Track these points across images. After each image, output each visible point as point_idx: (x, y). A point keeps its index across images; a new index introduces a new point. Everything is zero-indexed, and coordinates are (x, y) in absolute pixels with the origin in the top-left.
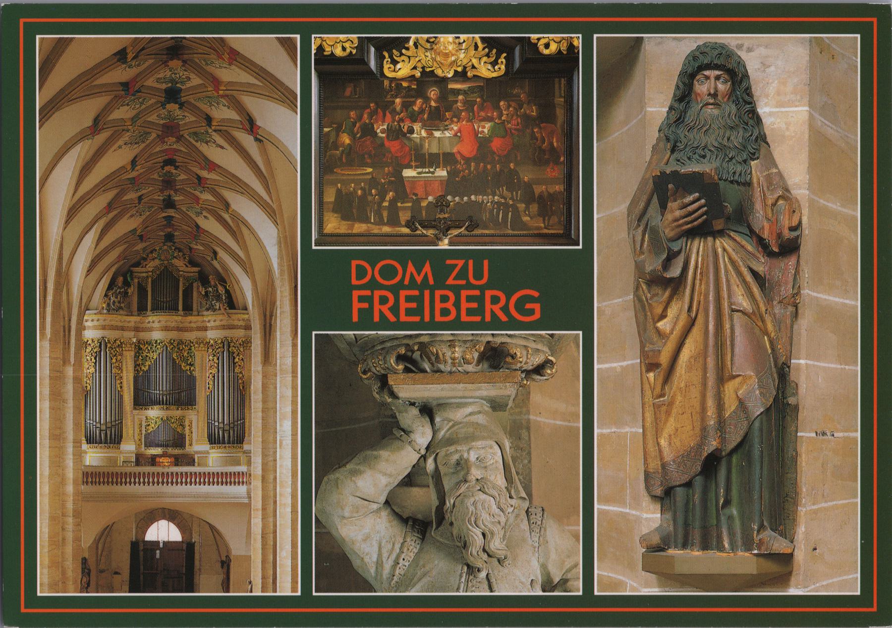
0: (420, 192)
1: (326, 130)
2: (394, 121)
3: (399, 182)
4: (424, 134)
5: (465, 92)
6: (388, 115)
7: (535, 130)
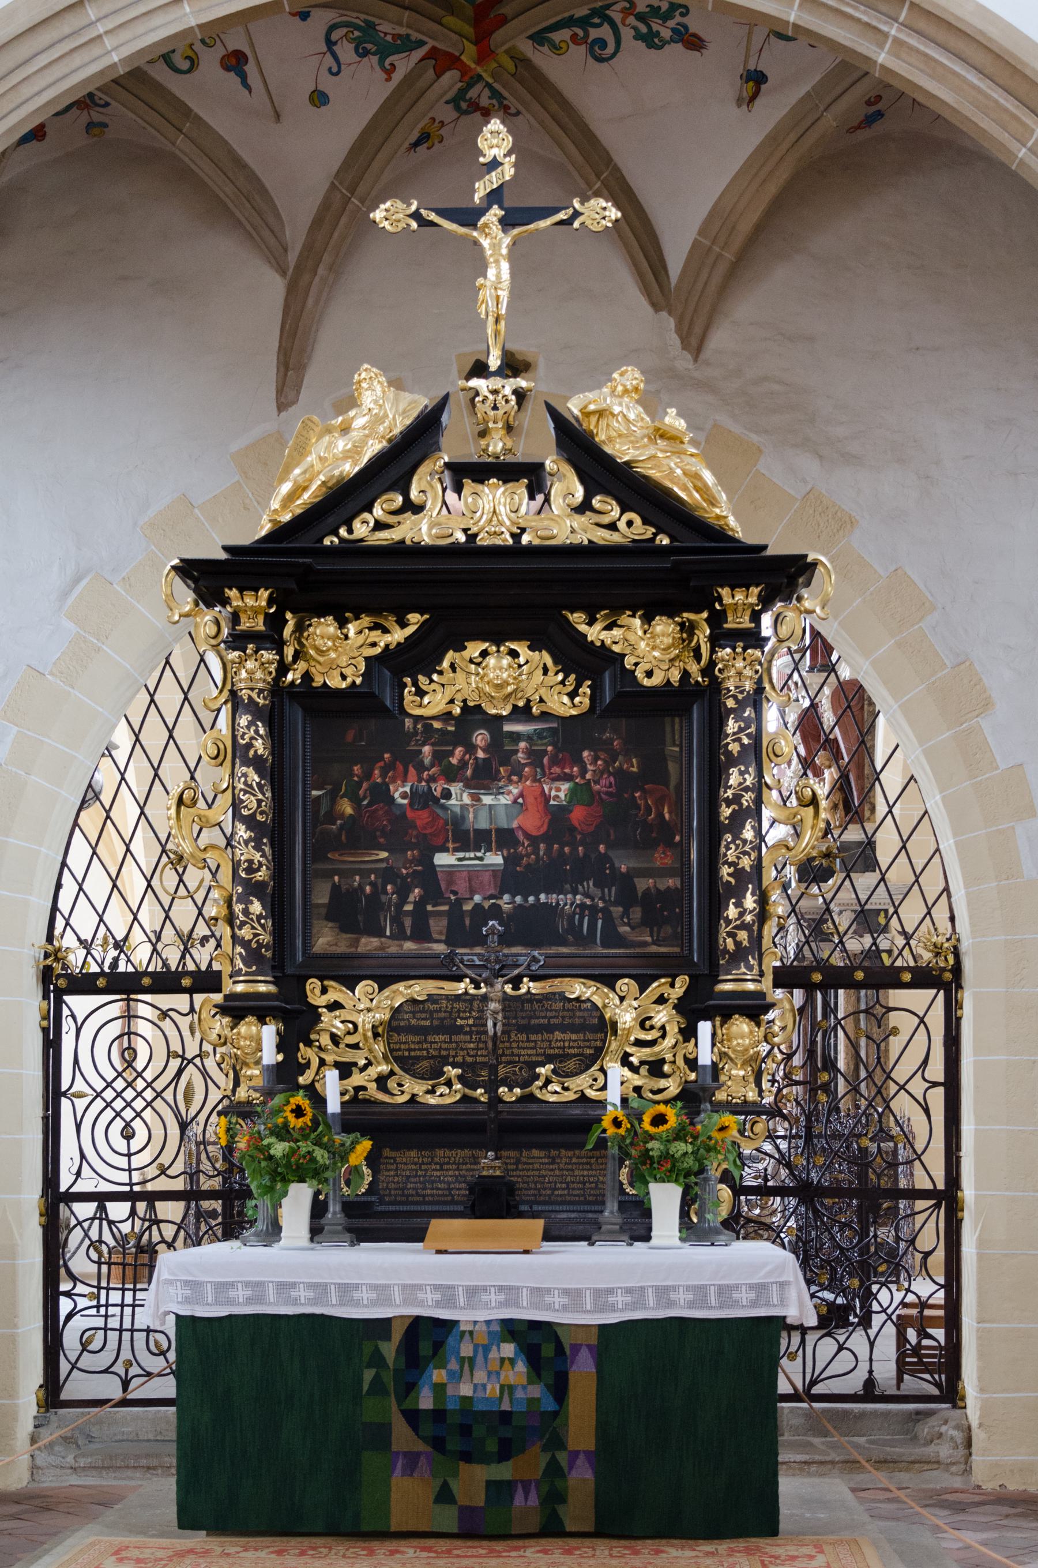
0: (462, 887)
1: (315, 793)
2: (420, 780)
3: (429, 875)
4: (467, 799)
5: (529, 738)
6: (412, 771)
7: (637, 795)
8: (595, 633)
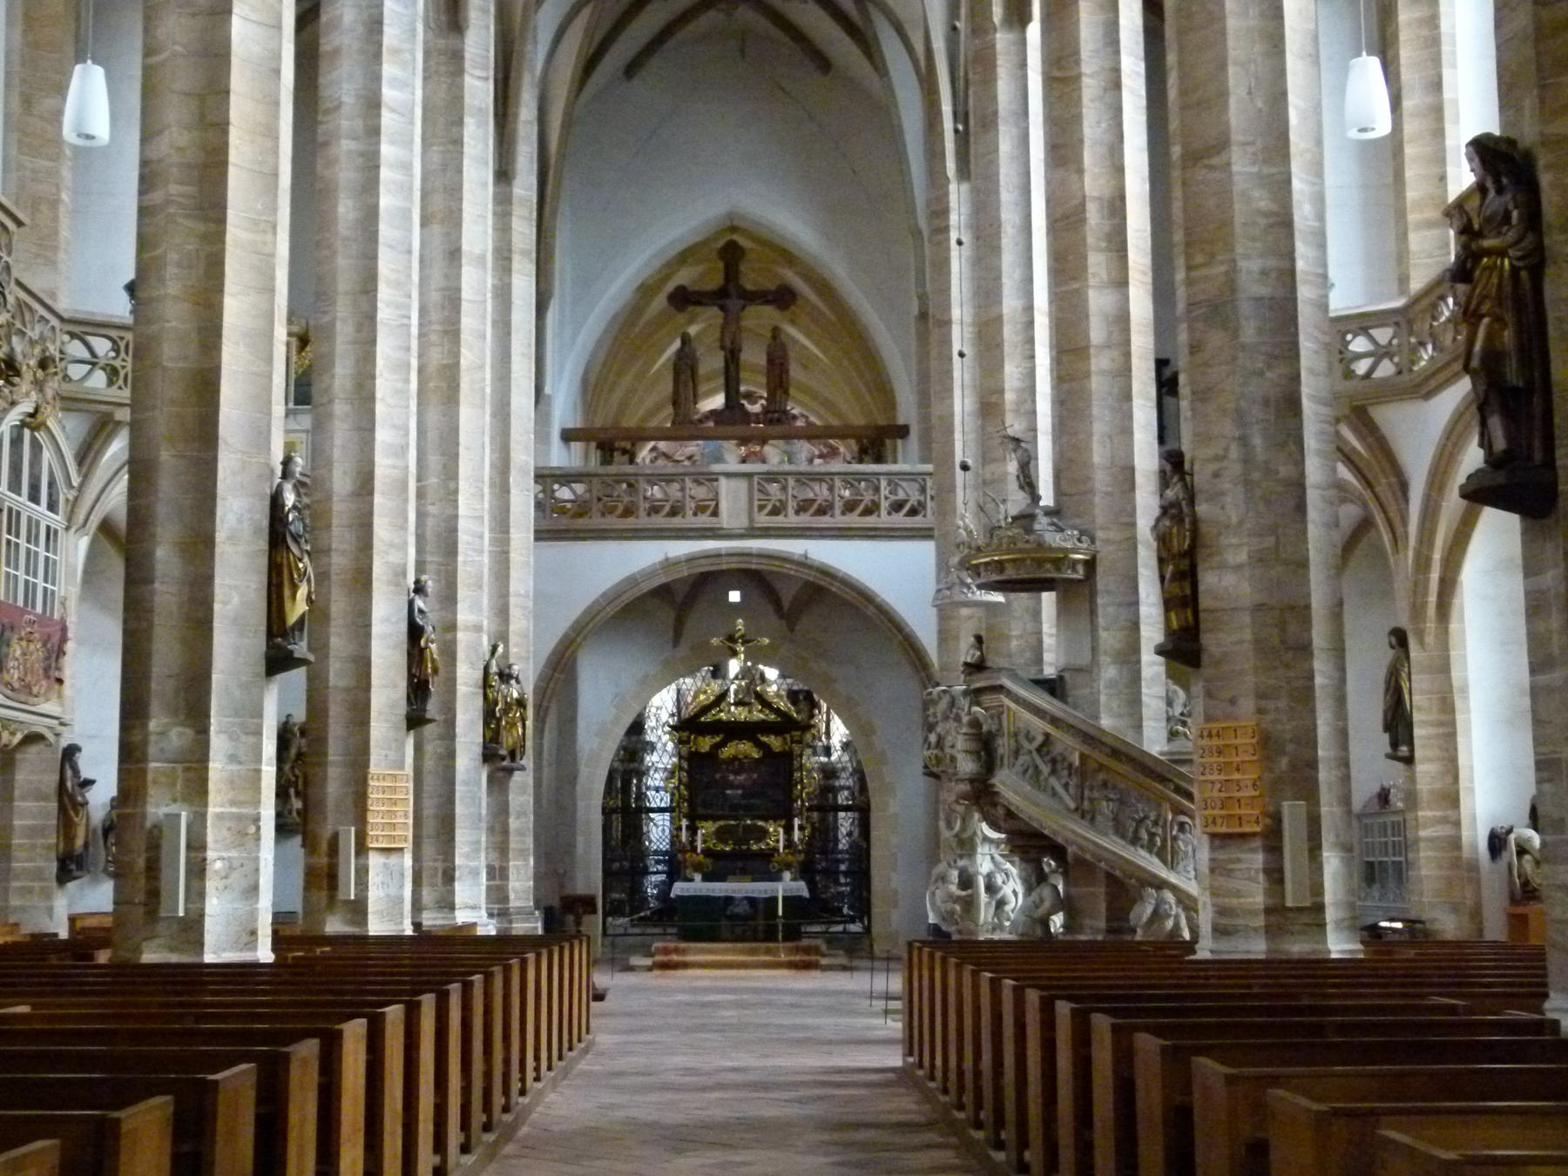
3: (725, 795)
8: (764, 739)
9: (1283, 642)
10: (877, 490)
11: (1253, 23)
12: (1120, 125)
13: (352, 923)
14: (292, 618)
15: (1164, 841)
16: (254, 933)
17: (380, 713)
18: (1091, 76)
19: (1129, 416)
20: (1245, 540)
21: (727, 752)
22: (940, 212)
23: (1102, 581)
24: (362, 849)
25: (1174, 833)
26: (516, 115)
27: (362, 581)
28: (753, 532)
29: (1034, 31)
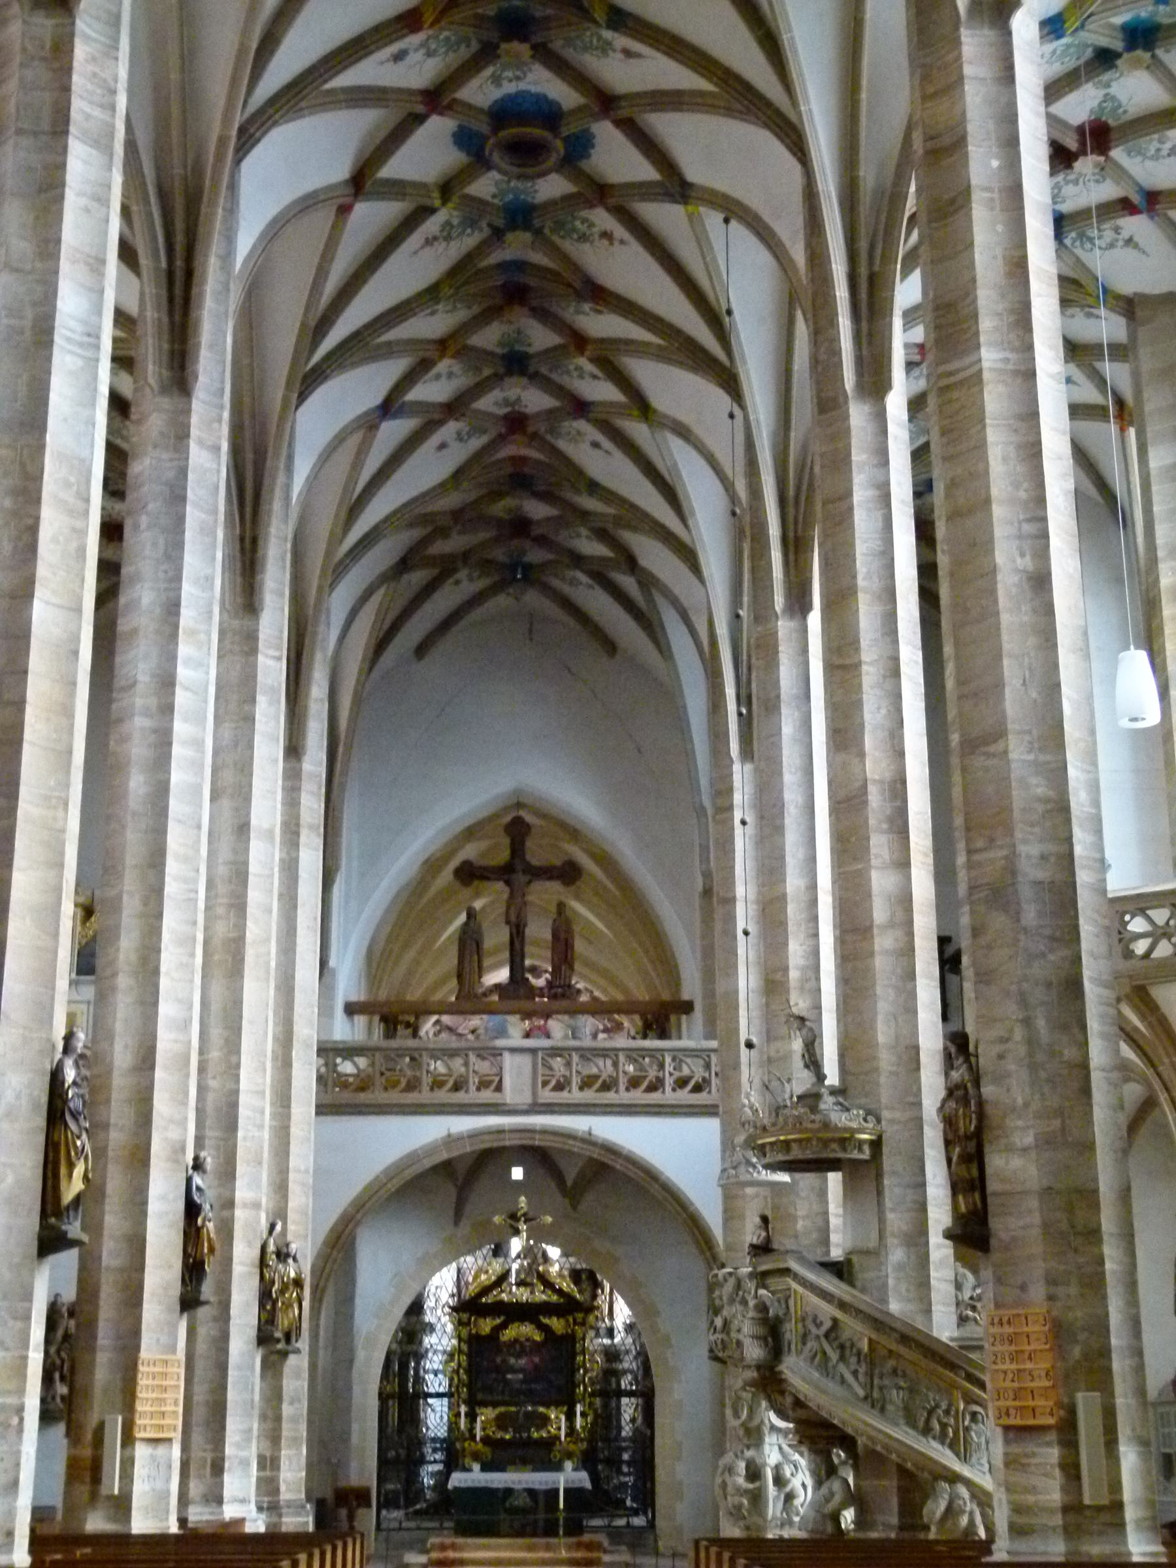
8: (546, 1321)
9: (1073, 1227)
10: (661, 1066)
11: (1026, 618)
12: (899, 710)
13: (115, 1520)
14: (68, 1196)
15: (956, 1432)
16: (10, 1534)
17: (153, 1294)
18: (870, 664)
19: (912, 995)
20: (1030, 1123)
21: (509, 1334)
22: (724, 791)
23: (889, 1161)
24: (128, 1439)
25: (966, 1423)
26: (307, 695)
27: (140, 1159)
28: (537, 1108)
29: (815, 619)
